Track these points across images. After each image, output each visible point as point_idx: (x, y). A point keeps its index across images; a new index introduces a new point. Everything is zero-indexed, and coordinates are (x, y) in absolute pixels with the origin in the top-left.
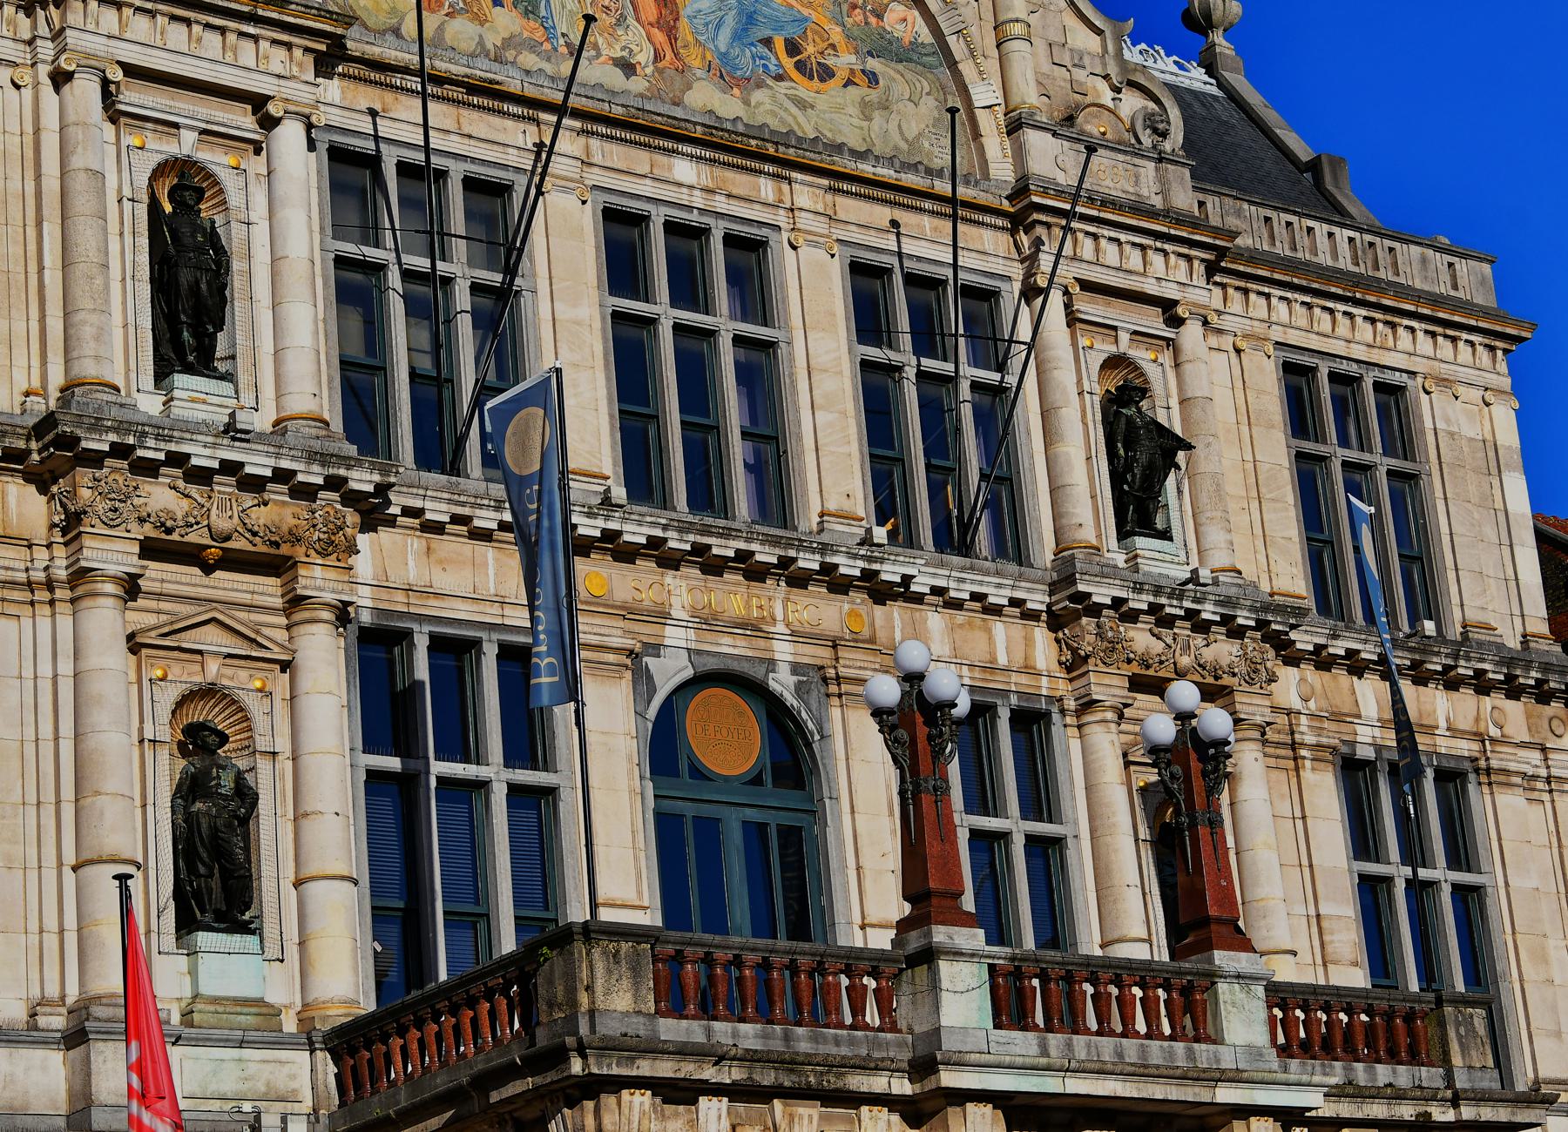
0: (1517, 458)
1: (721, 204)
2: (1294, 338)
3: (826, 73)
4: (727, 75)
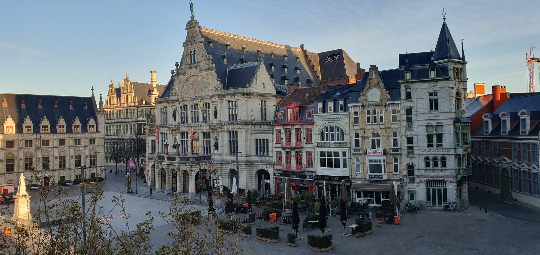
4: (198, 93)
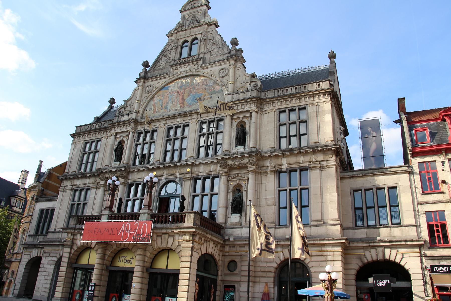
0: (330, 111)
1: (183, 122)
2: (280, 107)
3: (205, 99)
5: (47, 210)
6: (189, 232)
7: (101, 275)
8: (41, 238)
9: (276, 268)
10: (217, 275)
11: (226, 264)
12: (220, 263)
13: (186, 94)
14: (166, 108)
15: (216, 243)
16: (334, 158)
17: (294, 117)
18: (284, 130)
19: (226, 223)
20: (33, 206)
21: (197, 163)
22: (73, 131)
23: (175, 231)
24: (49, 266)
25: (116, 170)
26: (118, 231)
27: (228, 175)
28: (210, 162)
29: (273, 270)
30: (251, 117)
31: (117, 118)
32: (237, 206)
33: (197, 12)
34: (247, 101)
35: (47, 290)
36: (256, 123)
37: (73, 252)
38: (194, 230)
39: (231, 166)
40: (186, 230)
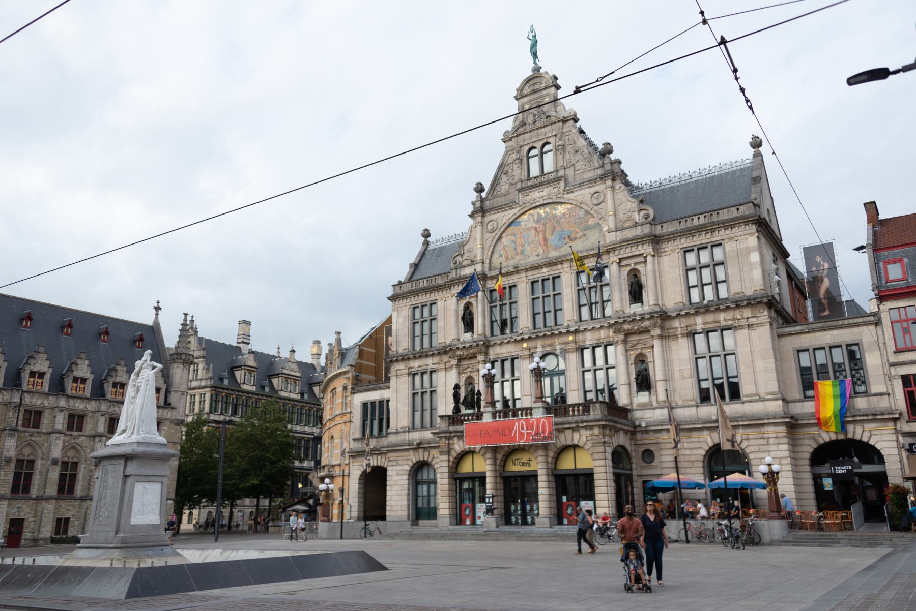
2: (685, 245)
4: (557, 248)
5: (373, 403)
6: (599, 426)
7: (496, 483)
8: (373, 443)
9: (705, 456)
10: (631, 469)
11: (640, 454)
12: (633, 454)
13: (548, 232)
14: (522, 252)
15: (626, 432)
16: (766, 313)
17: (705, 257)
18: (693, 277)
19: (631, 404)
20: (349, 398)
21: (582, 328)
22: (390, 293)
23: (581, 425)
24: (399, 478)
25: (471, 346)
26: (511, 432)
27: (625, 342)
28: (598, 326)
29: (701, 458)
30: (645, 262)
31: (454, 271)
32: (644, 382)
33: (543, 97)
34: (637, 241)
35: (405, 508)
36: (654, 271)
37: (452, 459)
38: (603, 423)
39: (628, 331)
40: (594, 424)
